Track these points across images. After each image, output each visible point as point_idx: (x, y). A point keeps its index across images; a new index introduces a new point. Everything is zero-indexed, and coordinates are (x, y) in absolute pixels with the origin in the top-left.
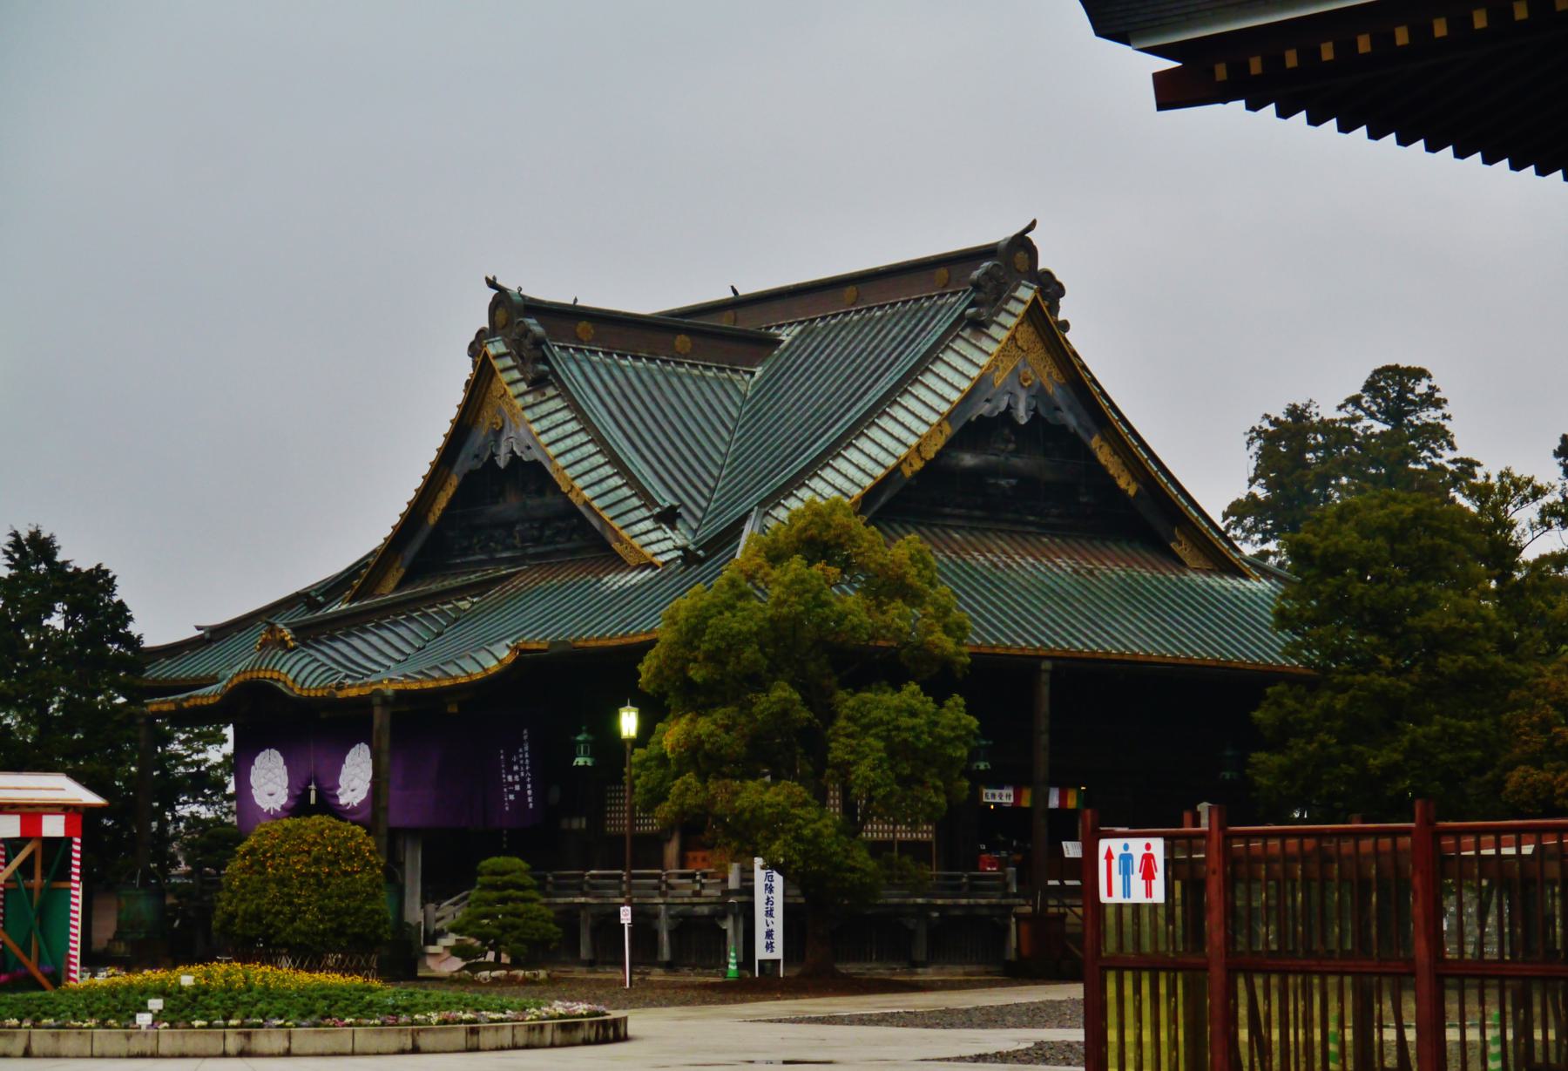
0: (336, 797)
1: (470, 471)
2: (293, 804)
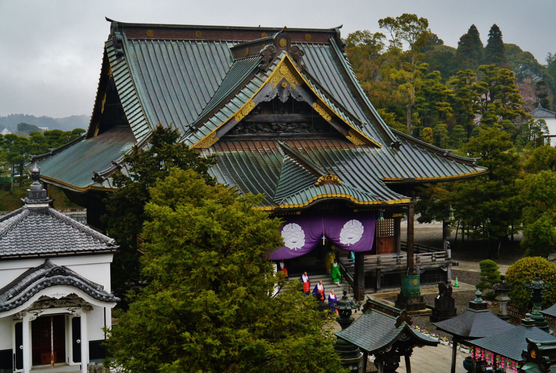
0: (339, 241)
1: (263, 102)
2: (309, 246)
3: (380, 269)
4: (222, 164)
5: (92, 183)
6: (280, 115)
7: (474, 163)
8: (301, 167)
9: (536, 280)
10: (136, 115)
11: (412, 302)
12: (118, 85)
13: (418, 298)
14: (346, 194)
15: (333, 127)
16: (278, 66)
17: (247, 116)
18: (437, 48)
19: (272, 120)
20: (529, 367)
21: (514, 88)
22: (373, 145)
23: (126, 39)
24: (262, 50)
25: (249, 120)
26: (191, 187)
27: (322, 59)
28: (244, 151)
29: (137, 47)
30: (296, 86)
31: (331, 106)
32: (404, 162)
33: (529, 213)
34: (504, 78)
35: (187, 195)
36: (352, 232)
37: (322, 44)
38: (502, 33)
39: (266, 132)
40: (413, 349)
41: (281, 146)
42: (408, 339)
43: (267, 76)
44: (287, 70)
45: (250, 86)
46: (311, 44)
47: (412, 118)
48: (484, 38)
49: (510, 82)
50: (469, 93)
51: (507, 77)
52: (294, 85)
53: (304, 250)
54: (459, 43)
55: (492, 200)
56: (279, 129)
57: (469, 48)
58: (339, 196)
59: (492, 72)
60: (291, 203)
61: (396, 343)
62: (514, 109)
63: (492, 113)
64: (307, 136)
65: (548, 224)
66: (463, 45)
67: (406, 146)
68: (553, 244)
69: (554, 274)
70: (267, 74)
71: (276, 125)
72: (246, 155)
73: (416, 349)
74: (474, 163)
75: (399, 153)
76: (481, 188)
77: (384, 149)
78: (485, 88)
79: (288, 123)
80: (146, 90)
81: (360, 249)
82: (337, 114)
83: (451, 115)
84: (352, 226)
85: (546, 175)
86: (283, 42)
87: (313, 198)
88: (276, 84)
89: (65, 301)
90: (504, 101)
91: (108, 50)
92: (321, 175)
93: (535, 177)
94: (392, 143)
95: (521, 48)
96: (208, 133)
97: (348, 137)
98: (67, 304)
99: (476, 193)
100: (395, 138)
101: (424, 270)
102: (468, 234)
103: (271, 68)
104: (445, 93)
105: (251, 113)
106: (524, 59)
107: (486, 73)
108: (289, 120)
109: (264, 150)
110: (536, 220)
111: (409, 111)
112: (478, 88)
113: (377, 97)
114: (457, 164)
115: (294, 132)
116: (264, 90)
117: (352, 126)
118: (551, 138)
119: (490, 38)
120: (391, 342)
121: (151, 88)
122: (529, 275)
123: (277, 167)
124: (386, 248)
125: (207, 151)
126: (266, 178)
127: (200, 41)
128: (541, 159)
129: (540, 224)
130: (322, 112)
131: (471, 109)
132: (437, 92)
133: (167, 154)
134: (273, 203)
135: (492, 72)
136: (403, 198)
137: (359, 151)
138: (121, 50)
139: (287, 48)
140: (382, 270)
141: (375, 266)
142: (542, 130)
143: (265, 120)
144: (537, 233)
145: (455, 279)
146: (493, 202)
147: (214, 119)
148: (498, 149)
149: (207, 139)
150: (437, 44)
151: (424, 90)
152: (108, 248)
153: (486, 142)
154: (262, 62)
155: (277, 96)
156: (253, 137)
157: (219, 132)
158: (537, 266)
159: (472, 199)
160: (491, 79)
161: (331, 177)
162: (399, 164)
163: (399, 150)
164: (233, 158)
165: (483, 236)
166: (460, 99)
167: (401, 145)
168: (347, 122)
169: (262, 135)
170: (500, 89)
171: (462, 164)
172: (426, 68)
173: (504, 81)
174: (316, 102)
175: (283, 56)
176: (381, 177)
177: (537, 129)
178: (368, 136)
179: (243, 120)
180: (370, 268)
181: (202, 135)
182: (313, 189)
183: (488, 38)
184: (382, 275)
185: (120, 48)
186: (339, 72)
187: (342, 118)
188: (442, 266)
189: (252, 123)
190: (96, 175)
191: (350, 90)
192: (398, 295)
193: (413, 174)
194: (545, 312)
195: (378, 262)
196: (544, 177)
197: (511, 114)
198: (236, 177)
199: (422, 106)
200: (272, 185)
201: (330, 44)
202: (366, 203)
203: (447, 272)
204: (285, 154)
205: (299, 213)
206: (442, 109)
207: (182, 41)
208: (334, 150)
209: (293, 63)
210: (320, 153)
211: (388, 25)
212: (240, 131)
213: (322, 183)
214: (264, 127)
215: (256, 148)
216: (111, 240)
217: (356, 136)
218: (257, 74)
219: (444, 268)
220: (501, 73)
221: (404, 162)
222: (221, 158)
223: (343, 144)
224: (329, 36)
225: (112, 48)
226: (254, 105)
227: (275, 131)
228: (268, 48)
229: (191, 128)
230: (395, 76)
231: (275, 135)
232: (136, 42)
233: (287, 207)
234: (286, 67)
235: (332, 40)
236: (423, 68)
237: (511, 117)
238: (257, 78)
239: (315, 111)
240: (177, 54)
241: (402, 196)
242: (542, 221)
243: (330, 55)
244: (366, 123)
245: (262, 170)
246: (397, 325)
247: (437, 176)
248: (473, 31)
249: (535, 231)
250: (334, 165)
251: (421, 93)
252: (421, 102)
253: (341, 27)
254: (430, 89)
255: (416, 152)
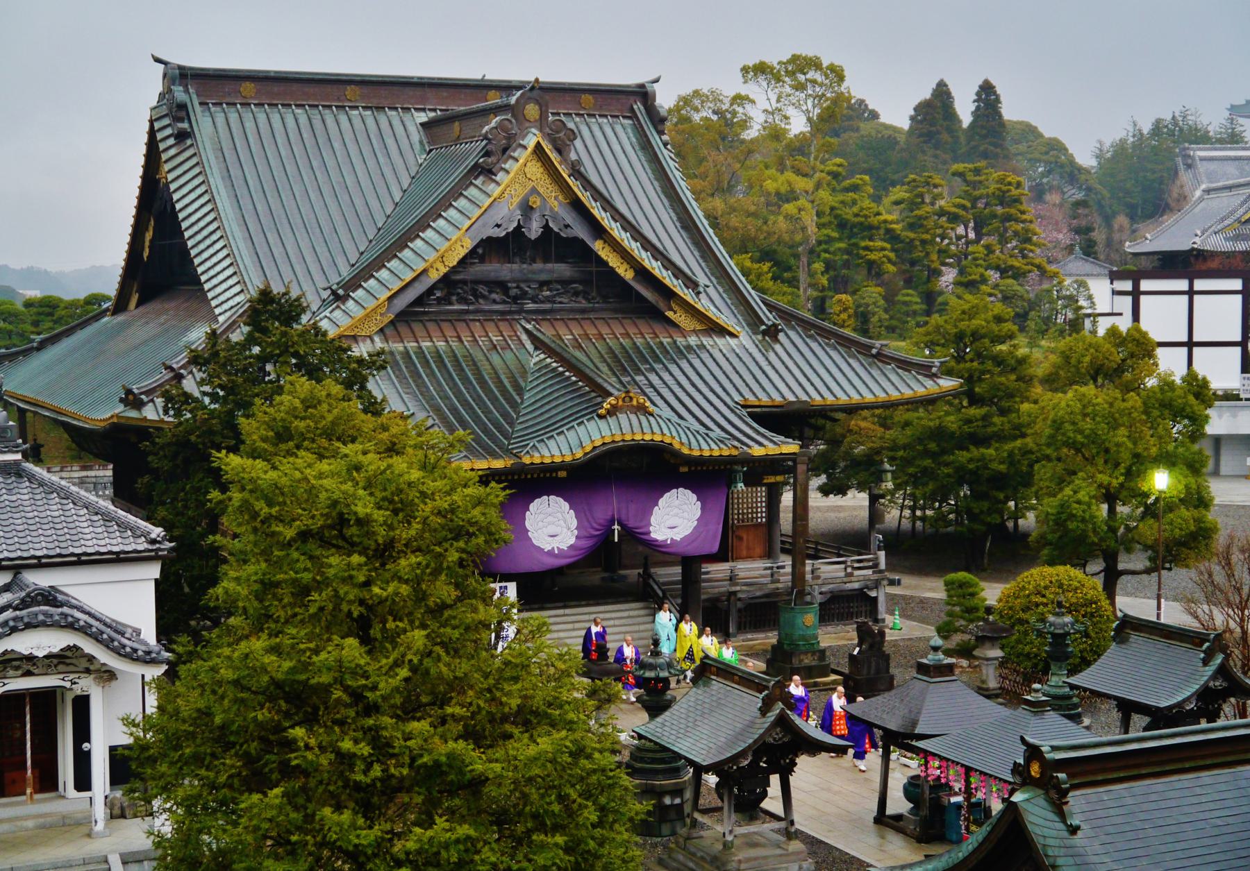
0: (649, 533)
2: (586, 543)
3: (735, 593)
4: (400, 370)
5: (120, 408)
6: (525, 266)
7: (934, 370)
8: (569, 378)
9: (1057, 614)
10: (215, 264)
11: (801, 661)
12: (178, 200)
13: (814, 653)
14: (663, 434)
15: (638, 294)
16: (521, 161)
17: (454, 267)
18: (866, 128)
19: (508, 278)
20: (1026, 796)
21: (1023, 212)
22: (722, 331)
23: (196, 102)
24: (486, 128)
25: (458, 277)
26: (330, 418)
27: (617, 148)
28: (447, 341)
29: (220, 119)
30: (560, 204)
31: (634, 247)
32: (787, 367)
33: (1048, 475)
34: (1004, 192)
35: (320, 435)
36: (676, 515)
37: (617, 117)
38: (1002, 99)
39: (494, 302)
40: (797, 760)
41: (527, 331)
42: (786, 740)
43: (498, 184)
44: (541, 170)
45: (461, 203)
46: (594, 116)
47: (811, 274)
48: (965, 110)
49: (1017, 201)
50: (930, 223)
51: (1009, 191)
52: (555, 202)
53: (573, 553)
54: (912, 118)
55: (972, 448)
56: (524, 295)
57: (933, 129)
58: (648, 437)
59: (978, 178)
60: (547, 453)
61: (761, 749)
62: (1024, 257)
63: (977, 266)
64: (583, 311)
65: (1087, 499)
66: (921, 122)
67: (792, 334)
68: (1096, 540)
69: (1096, 603)
70: (498, 178)
71: (518, 287)
72: (453, 351)
73: (803, 761)
74: (934, 370)
75: (777, 347)
76: (952, 422)
77: (745, 340)
78: (962, 213)
79: (543, 284)
80: (238, 211)
81: (692, 550)
82: (646, 264)
83: (891, 268)
84: (677, 502)
85: (1084, 395)
86: (532, 110)
87: (592, 442)
88: (516, 201)
89: (55, 661)
90: (1003, 241)
91: (157, 125)
92: (610, 395)
93: (1061, 399)
94: (764, 327)
95: (1041, 129)
96: (371, 304)
97: (669, 314)
98: (61, 668)
99: (939, 434)
100: (769, 318)
101: (829, 596)
102: (923, 519)
103: (507, 166)
104: (880, 223)
105: (462, 262)
106: (1047, 153)
107: (965, 181)
108: (544, 277)
109: (491, 341)
110: (1061, 490)
111: (804, 260)
112: (949, 213)
113: (736, 229)
114: (900, 371)
115: (554, 302)
116: (491, 212)
117: (678, 291)
118: (1100, 319)
119: (978, 108)
120: (750, 747)
121: (251, 207)
122: (1046, 605)
123: (517, 376)
124: (748, 548)
125: (368, 341)
126: (494, 400)
127: (356, 108)
128: (1073, 361)
129: (1069, 497)
130: (613, 261)
131: (934, 257)
132: (862, 219)
133: (279, 347)
134: (509, 452)
135: (978, 178)
136: (783, 443)
137: (692, 343)
138: (185, 125)
139: (541, 123)
140: (740, 595)
141: (725, 587)
142: (1082, 303)
143: (493, 276)
144: (1064, 516)
145: (893, 614)
146: (975, 452)
147: (383, 274)
148: (986, 340)
149: (367, 315)
150: (867, 119)
151: (836, 217)
152: (150, 547)
153: (963, 325)
154: (487, 154)
155: (519, 227)
156: (467, 312)
157: (395, 301)
158: (1061, 586)
159: (933, 446)
160: (977, 193)
161: (631, 399)
162: (777, 372)
163: (777, 341)
164: (425, 357)
165: (958, 522)
166: (912, 235)
167: (782, 330)
168: (667, 282)
169: (487, 308)
170: (995, 216)
171: (909, 371)
172: (840, 169)
173: (1003, 198)
174: (601, 238)
175: (531, 141)
176: (737, 398)
177: (1072, 299)
178: (712, 312)
179: (446, 276)
180: (716, 590)
181: (359, 307)
182: (592, 422)
183: (973, 108)
184: (739, 605)
185: (181, 120)
186: (652, 176)
187: (657, 273)
188: (867, 587)
189: (464, 282)
190: (129, 392)
191: (677, 214)
192: (773, 647)
193: (807, 393)
194: (1073, 680)
195: (732, 579)
196: (1080, 400)
197: (1018, 268)
198: (430, 399)
199: (832, 249)
200: (505, 415)
201: (633, 116)
202: (706, 454)
203: (876, 598)
204: (536, 348)
205: (562, 474)
206: (873, 256)
207: (317, 106)
208: (639, 341)
209: (553, 156)
210: (610, 348)
211: (761, 78)
212: (439, 300)
213: (613, 412)
214: (490, 292)
215: (473, 336)
216: (157, 532)
217: (686, 311)
218: (476, 178)
219: (871, 589)
220: (998, 182)
221: (787, 367)
222: (398, 358)
223: (658, 328)
224: (632, 98)
225: (166, 121)
226: (469, 244)
227: (515, 299)
228: (500, 126)
229: (334, 293)
230: (775, 185)
231: (514, 307)
232: (218, 109)
233: (537, 460)
234: (539, 164)
235: (639, 107)
236: (835, 168)
237: (1018, 275)
238: (476, 186)
239: (599, 258)
240: (305, 136)
241: (782, 438)
242: (1075, 492)
243: (634, 140)
244: (708, 283)
245: (486, 382)
246: (764, 710)
247: (856, 398)
248: (942, 94)
249: (1059, 513)
250: (638, 371)
251: (830, 222)
252: (830, 240)
253: (657, 81)
254: (848, 213)
255: (814, 345)
